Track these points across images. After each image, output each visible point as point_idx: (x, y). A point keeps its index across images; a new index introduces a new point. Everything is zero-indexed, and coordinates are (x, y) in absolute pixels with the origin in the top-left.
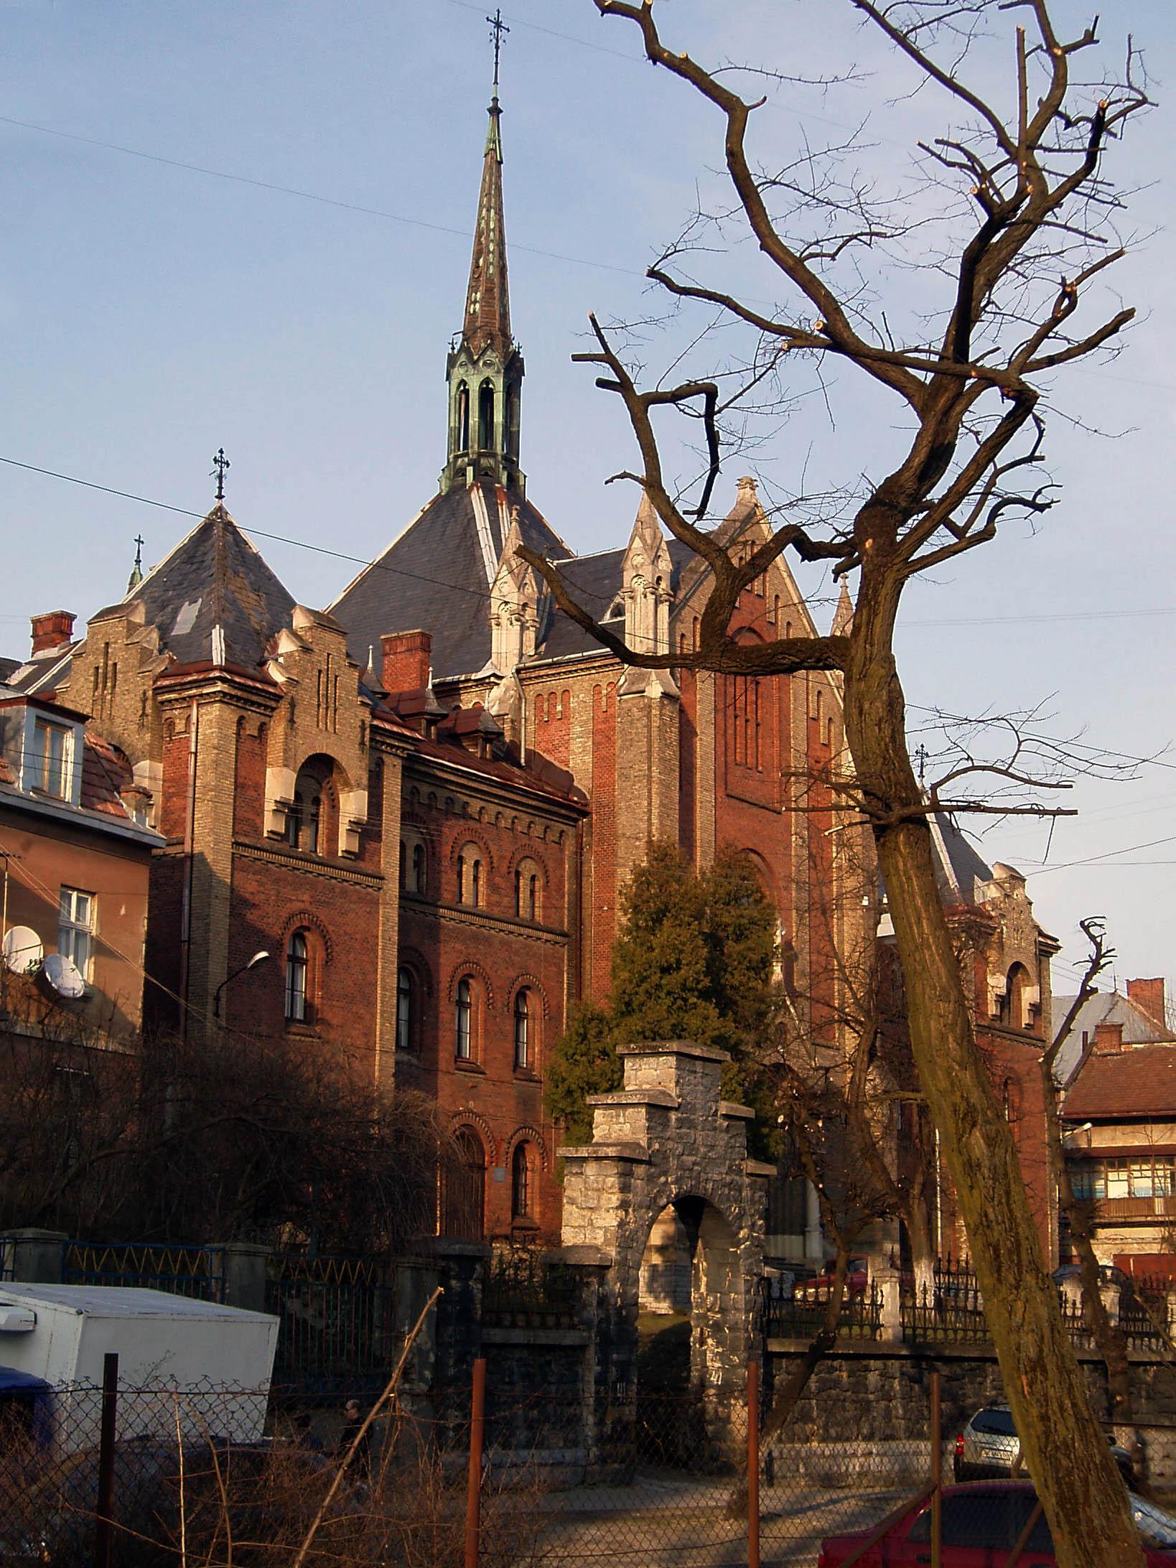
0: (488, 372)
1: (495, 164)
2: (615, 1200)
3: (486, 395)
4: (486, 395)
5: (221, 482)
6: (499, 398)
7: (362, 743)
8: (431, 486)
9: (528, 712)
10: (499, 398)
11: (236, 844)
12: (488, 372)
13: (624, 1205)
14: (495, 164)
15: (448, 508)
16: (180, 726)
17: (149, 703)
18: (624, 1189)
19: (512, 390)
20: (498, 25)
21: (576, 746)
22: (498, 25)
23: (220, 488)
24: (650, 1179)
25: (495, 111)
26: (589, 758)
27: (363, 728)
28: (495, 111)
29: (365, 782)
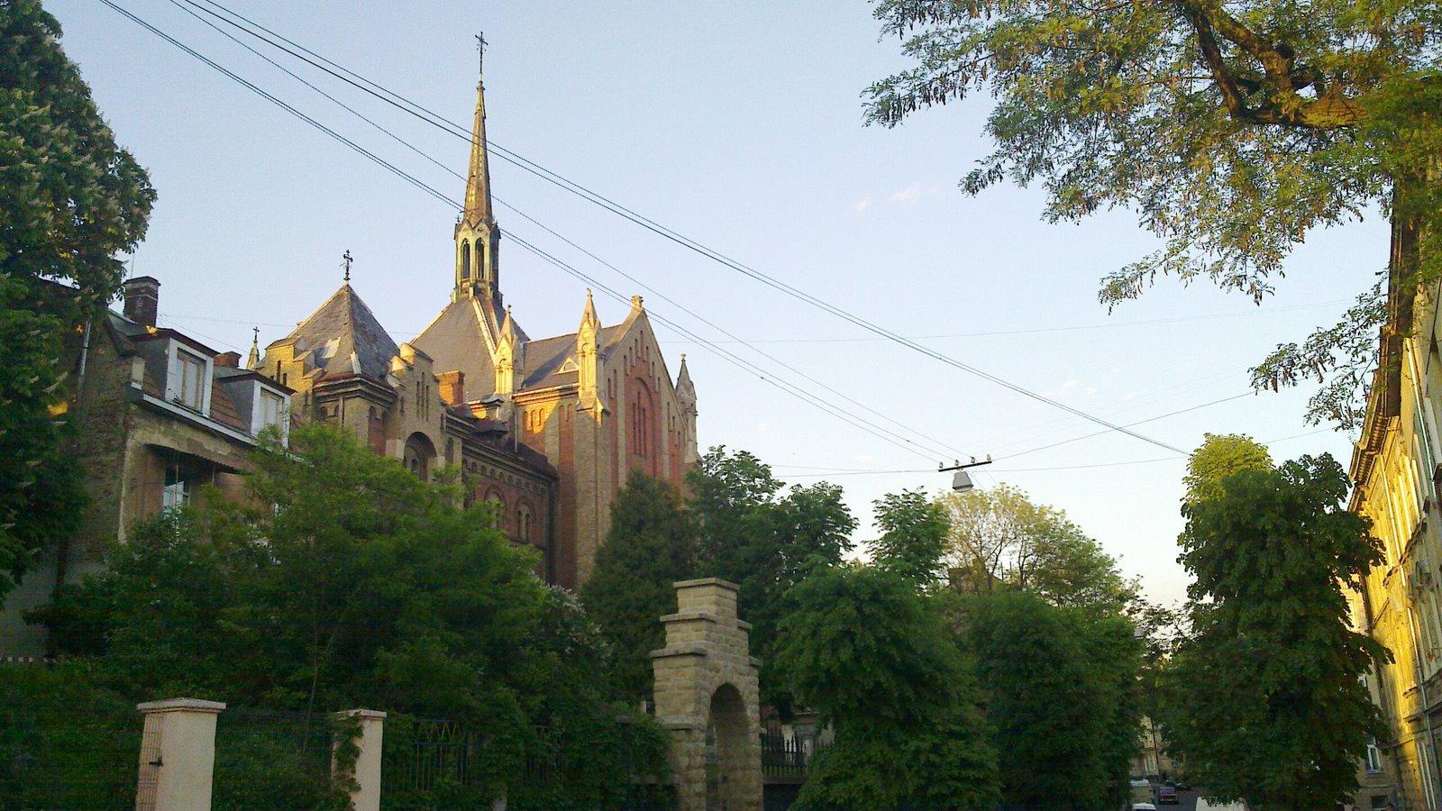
3: (479, 246)
4: (479, 246)
5: (347, 270)
6: (487, 250)
7: (442, 428)
8: (446, 296)
10: (487, 250)
15: (456, 309)
16: (331, 412)
17: (310, 398)
20: (482, 40)
22: (482, 40)
23: (347, 274)
26: (557, 447)
27: (442, 418)
29: (443, 451)
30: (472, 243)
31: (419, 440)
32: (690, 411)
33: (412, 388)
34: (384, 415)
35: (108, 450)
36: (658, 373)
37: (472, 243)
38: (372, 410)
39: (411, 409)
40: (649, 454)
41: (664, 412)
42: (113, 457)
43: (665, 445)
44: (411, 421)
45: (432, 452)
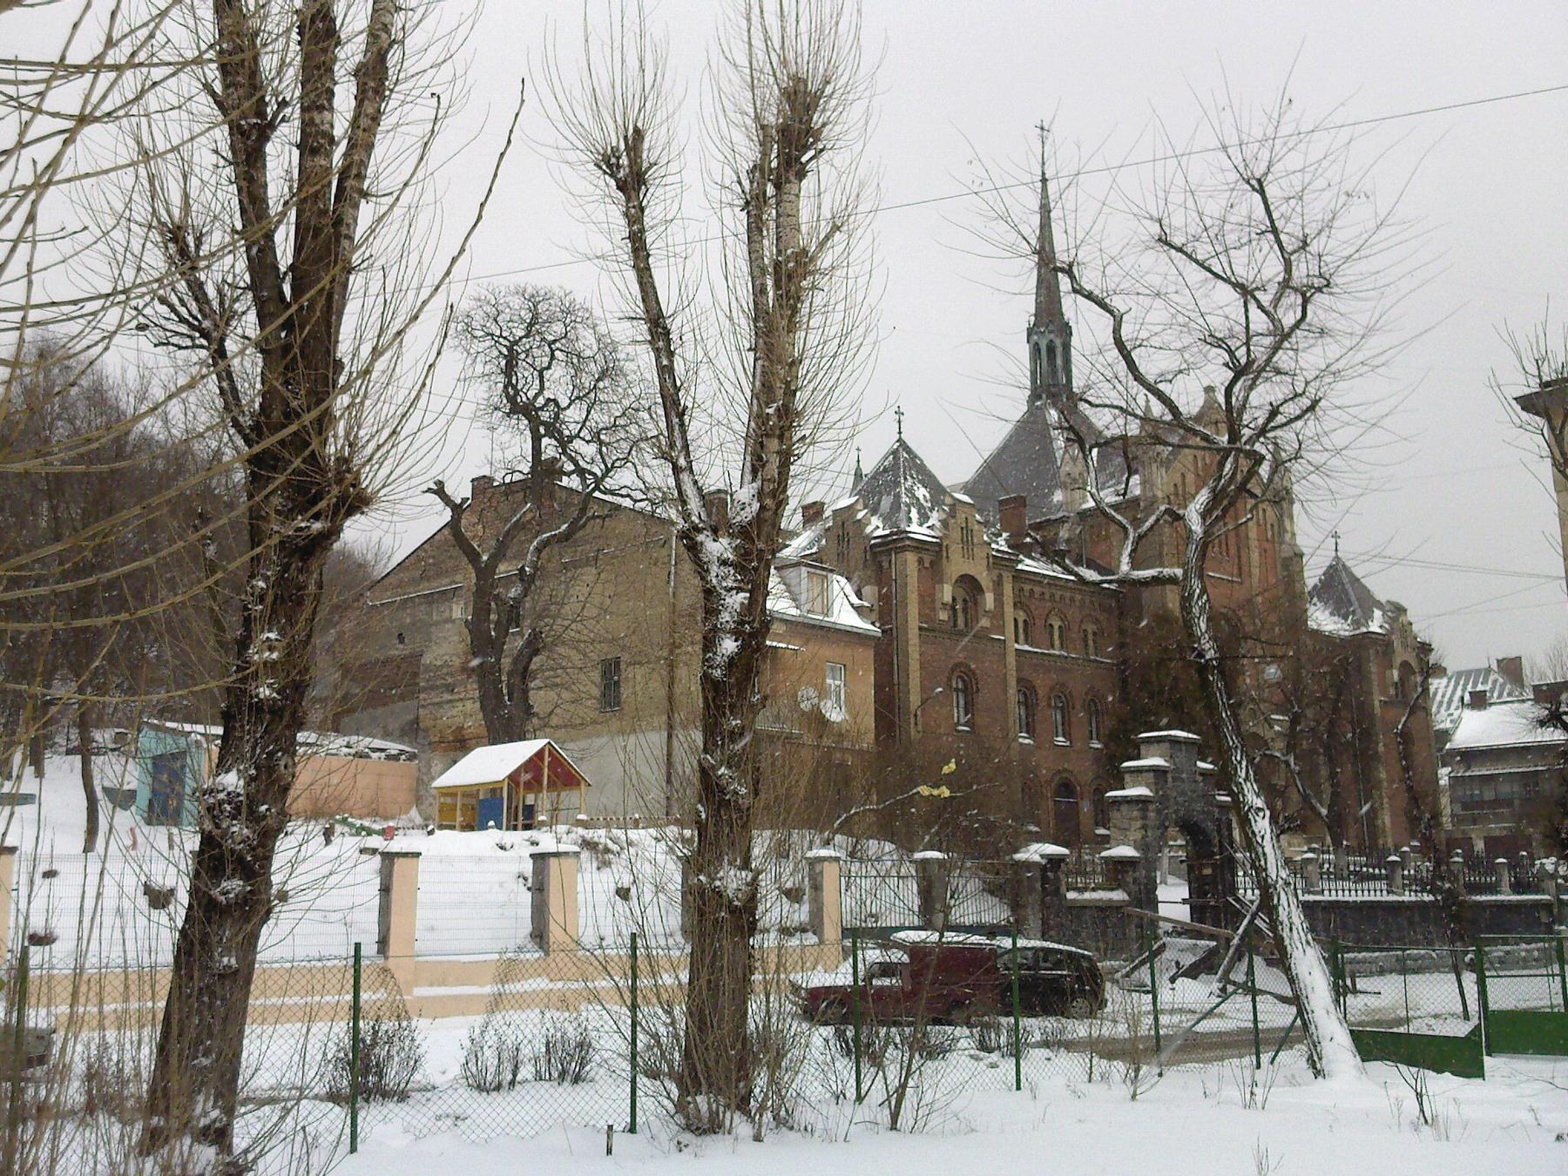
1: (1045, 210)
2: (1139, 824)
3: (1051, 349)
4: (1051, 349)
6: (1059, 351)
10: (1059, 351)
11: (920, 629)
13: (1144, 827)
14: (1045, 210)
16: (885, 564)
18: (1144, 818)
19: (1067, 347)
24: (1159, 812)
31: (969, 584)
33: (956, 534)
34: (931, 563)
38: (920, 561)
43: (1254, 543)
44: (957, 565)
45: (980, 590)
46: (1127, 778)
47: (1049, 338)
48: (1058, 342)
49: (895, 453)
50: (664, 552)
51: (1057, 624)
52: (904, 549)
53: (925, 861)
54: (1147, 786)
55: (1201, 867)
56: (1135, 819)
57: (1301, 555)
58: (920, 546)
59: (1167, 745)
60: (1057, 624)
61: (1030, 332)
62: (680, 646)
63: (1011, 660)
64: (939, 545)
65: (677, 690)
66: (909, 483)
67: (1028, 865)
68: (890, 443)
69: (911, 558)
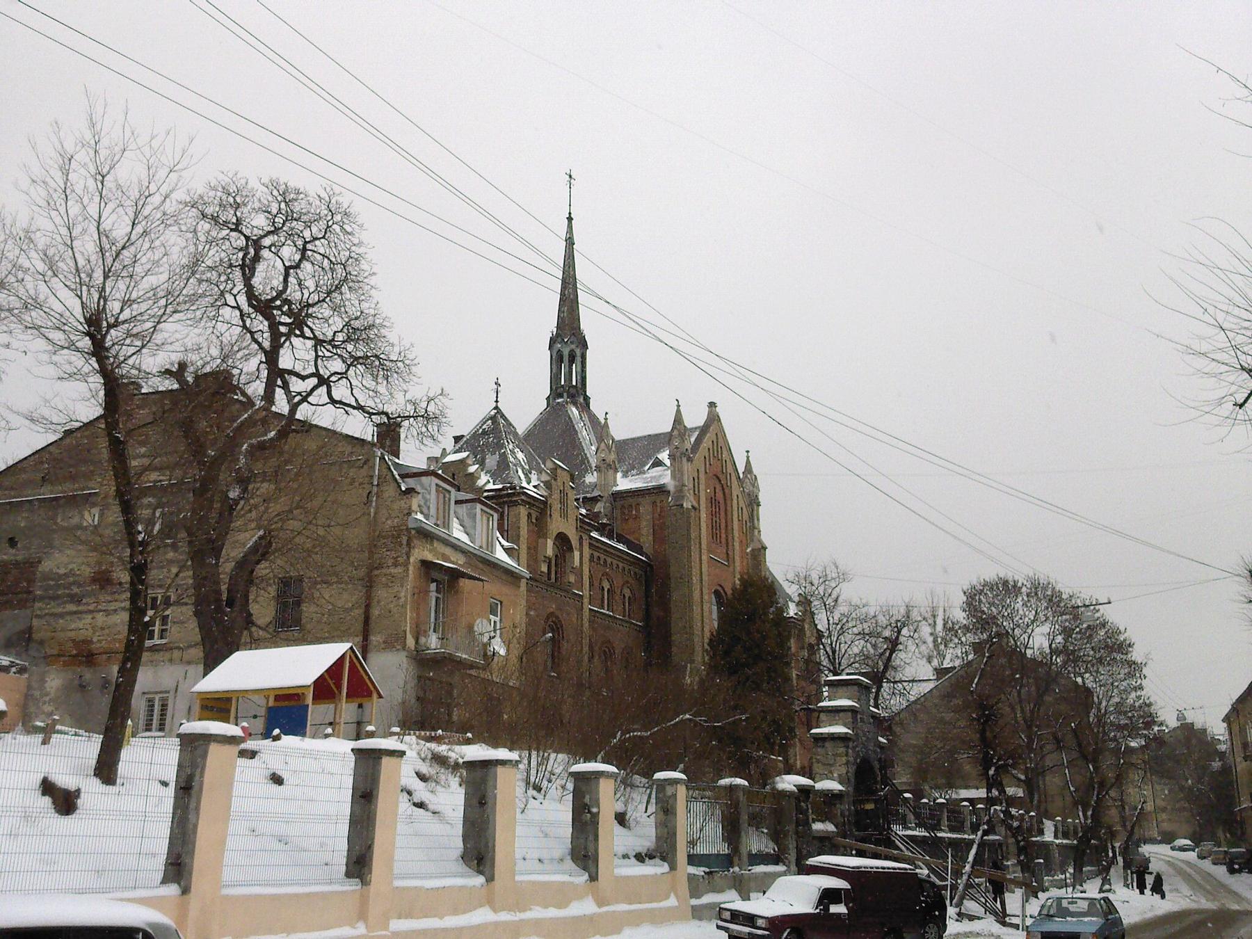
0: (573, 346)
1: (570, 242)
9: (617, 513)
12: (573, 346)
14: (570, 242)
21: (644, 531)
25: (570, 219)
26: (651, 538)
28: (570, 219)
30: (566, 353)
31: (562, 539)
32: (753, 502)
33: (556, 496)
35: (395, 565)
36: (730, 469)
37: (566, 353)
38: (529, 515)
39: (556, 515)
40: (723, 541)
41: (735, 501)
42: (400, 569)
43: (736, 534)
44: (558, 524)
45: (571, 549)
46: (823, 716)
47: (568, 344)
48: (578, 352)
49: (493, 418)
50: (364, 472)
51: (606, 586)
52: (515, 504)
53: (731, 788)
54: (845, 726)
55: (862, 802)
56: (840, 755)
57: (765, 548)
58: (531, 501)
59: (856, 688)
60: (606, 586)
61: (553, 342)
62: (380, 567)
63: (586, 614)
64: (545, 503)
65: (375, 612)
66: (511, 446)
67: (783, 794)
68: (487, 409)
69: (523, 511)
